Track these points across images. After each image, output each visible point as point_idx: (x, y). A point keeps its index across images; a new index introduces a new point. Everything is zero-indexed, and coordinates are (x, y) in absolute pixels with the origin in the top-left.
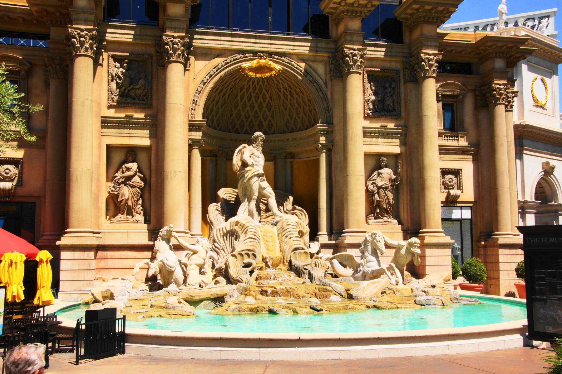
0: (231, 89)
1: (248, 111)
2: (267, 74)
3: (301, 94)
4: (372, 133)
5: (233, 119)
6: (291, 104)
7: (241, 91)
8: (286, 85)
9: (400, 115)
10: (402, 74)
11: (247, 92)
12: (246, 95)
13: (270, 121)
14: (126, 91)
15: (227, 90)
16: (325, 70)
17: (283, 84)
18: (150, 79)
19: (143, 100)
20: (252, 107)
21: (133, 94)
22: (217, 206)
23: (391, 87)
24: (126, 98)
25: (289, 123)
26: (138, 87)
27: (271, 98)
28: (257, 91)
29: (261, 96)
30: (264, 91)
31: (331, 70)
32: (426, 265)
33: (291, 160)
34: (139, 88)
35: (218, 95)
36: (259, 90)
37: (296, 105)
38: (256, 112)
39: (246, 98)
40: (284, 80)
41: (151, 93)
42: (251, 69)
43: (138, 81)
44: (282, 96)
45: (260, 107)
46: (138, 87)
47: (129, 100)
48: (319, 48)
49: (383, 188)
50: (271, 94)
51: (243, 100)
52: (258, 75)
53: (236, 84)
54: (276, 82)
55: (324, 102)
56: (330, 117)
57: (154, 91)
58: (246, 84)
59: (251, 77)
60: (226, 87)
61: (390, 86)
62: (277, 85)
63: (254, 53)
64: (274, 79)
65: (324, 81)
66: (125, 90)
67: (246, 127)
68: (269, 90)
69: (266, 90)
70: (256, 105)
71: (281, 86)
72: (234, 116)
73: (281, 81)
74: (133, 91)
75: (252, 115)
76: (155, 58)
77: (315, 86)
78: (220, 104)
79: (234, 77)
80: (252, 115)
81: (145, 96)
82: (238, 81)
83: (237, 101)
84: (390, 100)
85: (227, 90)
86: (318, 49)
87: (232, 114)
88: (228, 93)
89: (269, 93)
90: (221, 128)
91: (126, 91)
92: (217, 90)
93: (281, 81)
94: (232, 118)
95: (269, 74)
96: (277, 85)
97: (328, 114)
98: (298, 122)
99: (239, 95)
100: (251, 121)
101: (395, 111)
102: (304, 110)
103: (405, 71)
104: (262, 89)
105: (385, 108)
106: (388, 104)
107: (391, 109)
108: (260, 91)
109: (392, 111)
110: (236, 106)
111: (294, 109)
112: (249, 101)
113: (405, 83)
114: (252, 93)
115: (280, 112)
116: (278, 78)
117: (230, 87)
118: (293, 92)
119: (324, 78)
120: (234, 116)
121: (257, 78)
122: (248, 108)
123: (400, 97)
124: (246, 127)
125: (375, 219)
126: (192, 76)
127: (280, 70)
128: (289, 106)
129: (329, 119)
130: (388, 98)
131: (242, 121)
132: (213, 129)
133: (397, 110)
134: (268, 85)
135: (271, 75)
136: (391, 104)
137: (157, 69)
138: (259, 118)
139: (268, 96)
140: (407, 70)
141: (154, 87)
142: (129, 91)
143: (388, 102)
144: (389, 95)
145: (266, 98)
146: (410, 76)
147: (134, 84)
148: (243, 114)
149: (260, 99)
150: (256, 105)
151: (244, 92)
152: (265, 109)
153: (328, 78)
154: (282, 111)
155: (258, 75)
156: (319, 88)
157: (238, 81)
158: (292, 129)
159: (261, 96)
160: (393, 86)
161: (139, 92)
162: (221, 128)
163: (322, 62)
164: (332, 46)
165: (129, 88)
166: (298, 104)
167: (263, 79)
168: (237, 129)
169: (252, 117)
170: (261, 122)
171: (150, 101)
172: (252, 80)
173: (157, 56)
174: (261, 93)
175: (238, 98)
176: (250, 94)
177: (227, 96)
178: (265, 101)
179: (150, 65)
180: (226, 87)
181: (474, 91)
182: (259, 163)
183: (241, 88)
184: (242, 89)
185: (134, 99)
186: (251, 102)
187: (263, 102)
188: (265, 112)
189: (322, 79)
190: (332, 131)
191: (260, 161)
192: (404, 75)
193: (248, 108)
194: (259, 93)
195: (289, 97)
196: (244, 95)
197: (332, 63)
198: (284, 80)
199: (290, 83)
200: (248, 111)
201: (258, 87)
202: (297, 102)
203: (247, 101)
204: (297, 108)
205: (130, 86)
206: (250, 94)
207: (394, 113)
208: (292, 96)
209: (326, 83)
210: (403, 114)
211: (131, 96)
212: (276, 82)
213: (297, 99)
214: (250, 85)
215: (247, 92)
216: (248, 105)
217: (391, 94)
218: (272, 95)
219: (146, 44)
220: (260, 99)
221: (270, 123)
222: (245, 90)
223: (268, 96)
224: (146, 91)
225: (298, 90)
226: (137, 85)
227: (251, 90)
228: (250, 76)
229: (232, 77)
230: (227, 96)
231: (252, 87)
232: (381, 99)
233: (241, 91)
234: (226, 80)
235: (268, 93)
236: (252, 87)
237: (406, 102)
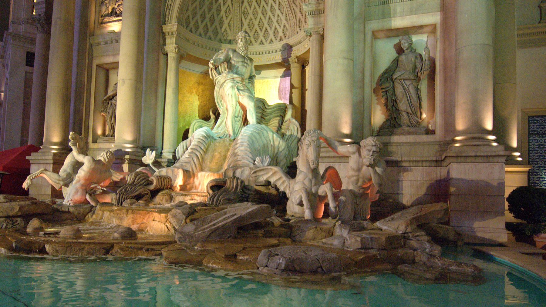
20: (264, 12)
22: (199, 123)
80: (265, 22)
87: (242, 25)
110: (246, 14)
132: (218, 42)
148: (256, 23)
150: (268, 9)
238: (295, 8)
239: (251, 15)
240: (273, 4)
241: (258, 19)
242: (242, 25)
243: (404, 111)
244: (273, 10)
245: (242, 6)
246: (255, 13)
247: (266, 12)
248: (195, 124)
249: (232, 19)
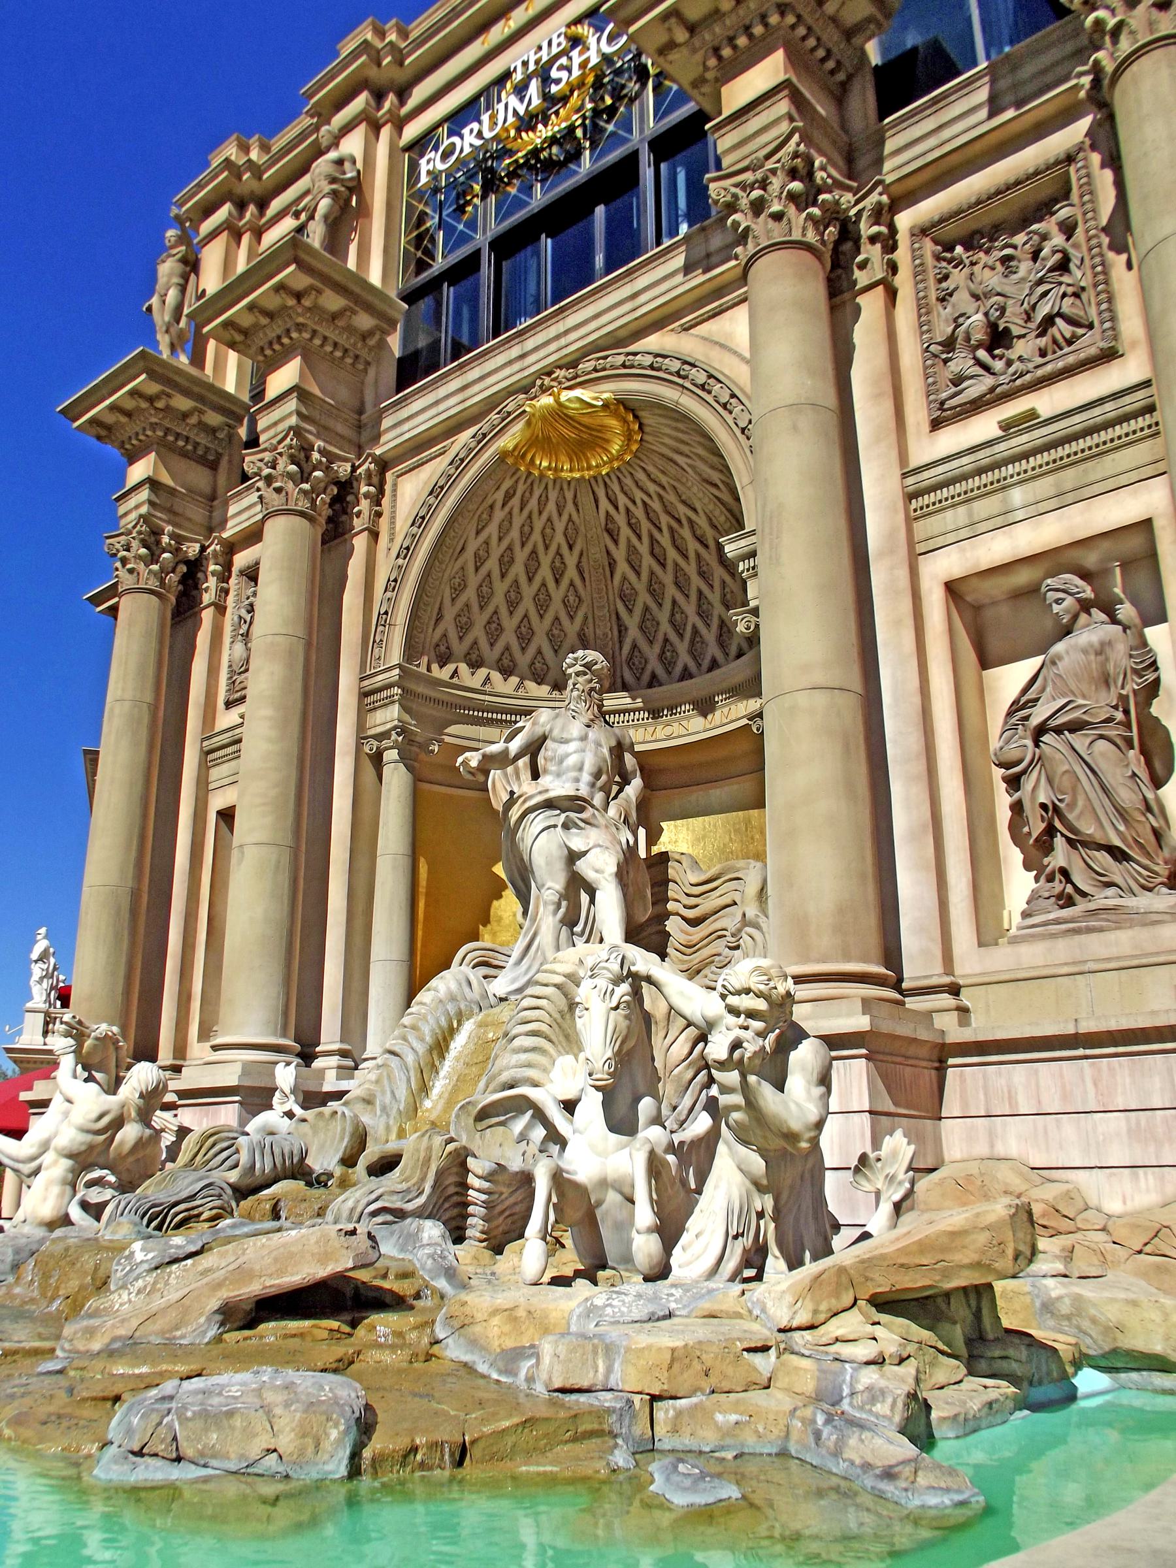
4: (964, 477)
5: (635, 646)
49: (1058, 731)
72: (633, 633)
82: (570, 507)
87: (622, 629)
88: (571, 560)
99: (620, 554)
110: (627, 598)
120: (633, 633)
125: (1062, 907)
148: (663, 616)
175: (622, 567)
177: (571, 573)
182: (565, 764)
183: (608, 531)
191: (568, 755)
196: (632, 550)
210: (1131, 324)
229: (533, 504)
230: (571, 573)
234: (518, 521)
241: (667, 605)
242: (620, 632)
244: (704, 568)
245: (612, 576)
247: (688, 579)
249: (590, 620)
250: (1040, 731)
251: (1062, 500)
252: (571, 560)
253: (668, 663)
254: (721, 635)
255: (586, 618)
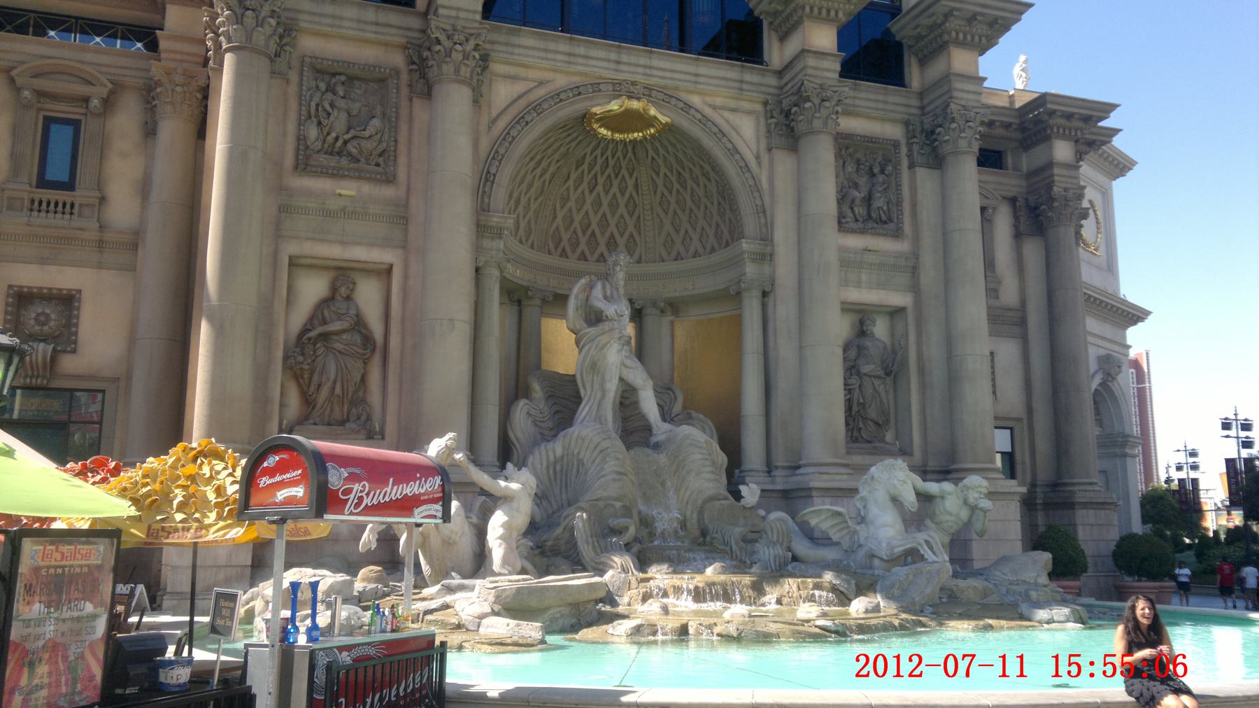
0: (558, 161)
1: (587, 213)
2: (636, 135)
3: (702, 180)
5: (557, 229)
6: (677, 202)
7: (577, 168)
8: (672, 159)
9: (903, 231)
10: (904, 150)
11: (589, 172)
12: (586, 179)
13: (631, 236)
14: (339, 144)
15: (550, 163)
16: (757, 130)
17: (665, 158)
18: (394, 119)
19: (378, 165)
20: (598, 203)
21: (354, 151)
22: (527, 406)
23: (883, 173)
24: (338, 158)
25: (672, 240)
26: (367, 134)
27: (636, 186)
28: (609, 170)
29: (616, 183)
30: (624, 171)
31: (769, 131)
32: (971, 540)
33: (672, 318)
34: (370, 137)
35: (533, 171)
36: (614, 168)
37: (689, 202)
38: (604, 214)
39: (584, 186)
40: (670, 149)
41: (395, 151)
42: (607, 120)
43: (368, 123)
44: (660, 182)
45: (614, 205)
46: (367, 134)
47: (344, 162)
48: (747, 83)
49: (870, 376)
50: (637, 179)
51: (580, 190)
52: (617, 136)
53: (571, 150)
54: (651, 153)
55: (756, 194)
56: (766, 226)
57: (402, 147)
58: (589, 153)
59: (603, 138)
60: (550, 156)
61: (882, 172)
62: (653, 159)
63: (617, 84)
64: (649, 148)
65: (755, 152)
66: (337, 139)
67: (583, 246)
68: (634, 169)
69: (628, 169)
70: (605, 201)
71: (661, 162)
73: (662, 151)
74: (355, 143)
75: (595, 220)
76: (405, 77)
77: (737, 161)
78: (532, 191)
79: (569, 135)
80: (595, 220)
81: (380, 155)
82: (573, 144)
83: (568, 189)
84: (882, 199)
85: (550, 163)
86: (745, 86)
87: (555, 217)
88: (552, 169)
89: (635, 175)
90: (532, 244)
91: (339, 144)
92: (532, 159)
93: (662, 151)
94: (554, 226)
95: (641, 134)
96: (653, 159)
97: (763, 221)
98: (691, 239)
99: (573, 176)
100: (593, 233)
101: (891, 221)
102: (706, 214)
103: (912, 143)
104: (621, 167)
105: (874, 215)
106: (878, 208)
107: (884, 218)
108: (614, 172)
109: (885, 223)
110: (565, 200)
111: (684, 211)
112: (591, 191)
113: (912, 166)
114: (599, 176)
115: (653, 218)
116: (658, 145)
117: (556, 156)
118: (686, 175)
119: (754, 147)
120: (559, 220)
121: (613, 140)
122: (588, 206)
123: (901, 194)
124: (583, 246)
125: (853, 442)
126: (485, 120)
127: (667, 123)
128: (673, 206)
129: (764, 230)
130: (878, 195)
131: (575, 232)
133: (895, 220)
134: (633, 159)
135: (644, 137)
136: (885, 208)
137: (411, 100)
138: (609, 230)
139: (631, 183)
140: (915, 140)
141: (402, 139)
142: (345, 142)
143: (879, 202)
144: (880, 189)
145: (626, 187)
146: (923, 152)
147: (358, 129)
148: (578, 218)
149: (615, 189)
150: (605, 201)
151: (583, 172)
152: (622, 209)
153: (763, 146)
154: (658, 215)
155: (617, 136)
156: (746, 165)
157: (573, 144)
158: (679, 253)
159: (616, 183)
160: (886, 172)
161: (368, 145)
162: (532, 244)
163: (750, 113)
164: (772, 81)
165: (347, 137)
166: (693, 201)
167: (623, 142)
168: (564, 249)
169: (594, 226)
170: (612, 236)
171: (392, 168)
172: (602, 145)
173: (411, 70)
174: (617, 176)
175: (571, 183)
176: (595, 176)
177: (547, 176)
178: (623, 195)
179: (395, 91)
180: (550, 156)
181: (1013, 201)
183: (578, 162)
184: (579, 164)
185: (358, 161)
186: (595, 193)
187: (618, 195)
188: (622, 216)
189: (750, 149)
190: (771, 255)
192: (910, 150)
193: (588, 206)
194: (613, 176)
195: (676, 186)
197: (772, 117)
198: (670, 149)
199: (680, 155)
200: (587, 213)
201: (611, 163)
202: (692, 195)
203: (587, 192)
204: (691, 210)
205: (347, 132)
206: (595, 176)
207: (892, 226)
208: (683, 184)
209: (758, 157)
210: (907, 228)
211: (350, 154)
212: (651, 153)
213: (692, 189)
214: (596, 157)
215: (589, 172)
216: (589, 199)
217: (884, 187)
218: (639, 181)
219: (386, 44)
220: (615, 189)
221: (631, 240)
222: (585, 167)
223: (631, 183)
224: (384, 145)
225: (697, 171)
226: (364, 130)
227: (597, 168)
228: (600, 136)
230: (547, 176)
231: (600, 161)
232: (864, 198)
233: (577, 168)
235: (631, 175)
236: (600, 161)
237: (914, 205)
238: (662, 215)
239: (572, 204)
240: (618, 195)
243: (872, 421)
246: (581, 202)
247: (600, 205)
248: (522, 409)
250: (865, 374)
251: (881, 286)
252: (552, 169)
253: (575, 244)
254: (609, 242)
255: (541, 203)
